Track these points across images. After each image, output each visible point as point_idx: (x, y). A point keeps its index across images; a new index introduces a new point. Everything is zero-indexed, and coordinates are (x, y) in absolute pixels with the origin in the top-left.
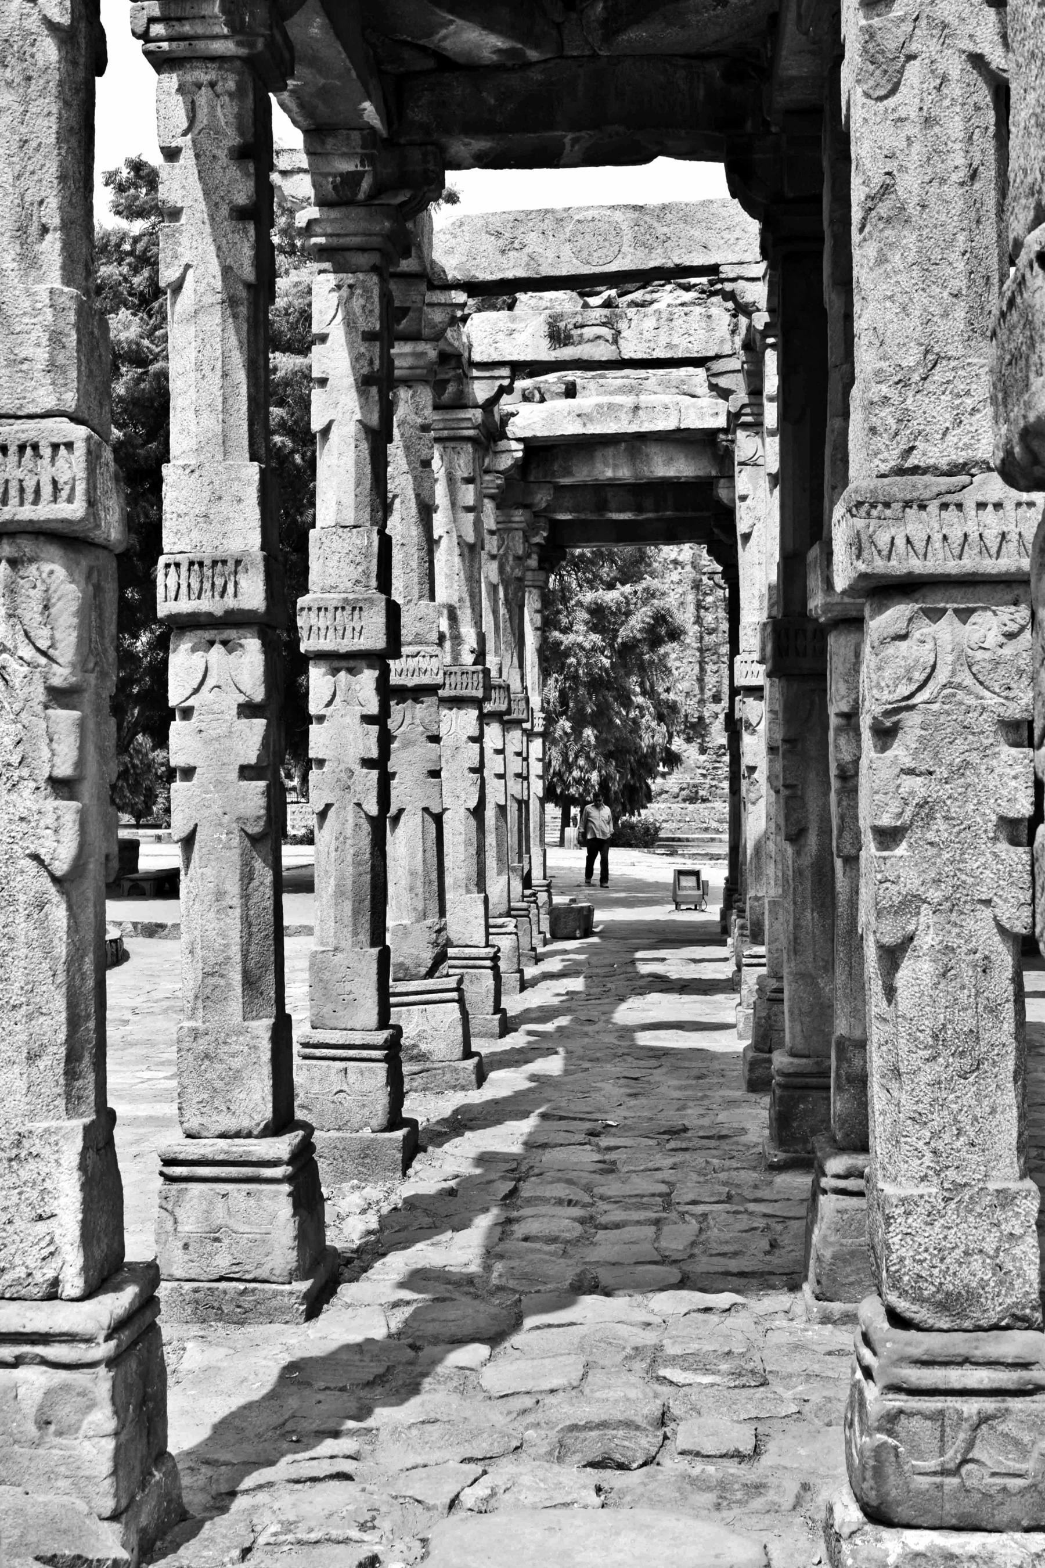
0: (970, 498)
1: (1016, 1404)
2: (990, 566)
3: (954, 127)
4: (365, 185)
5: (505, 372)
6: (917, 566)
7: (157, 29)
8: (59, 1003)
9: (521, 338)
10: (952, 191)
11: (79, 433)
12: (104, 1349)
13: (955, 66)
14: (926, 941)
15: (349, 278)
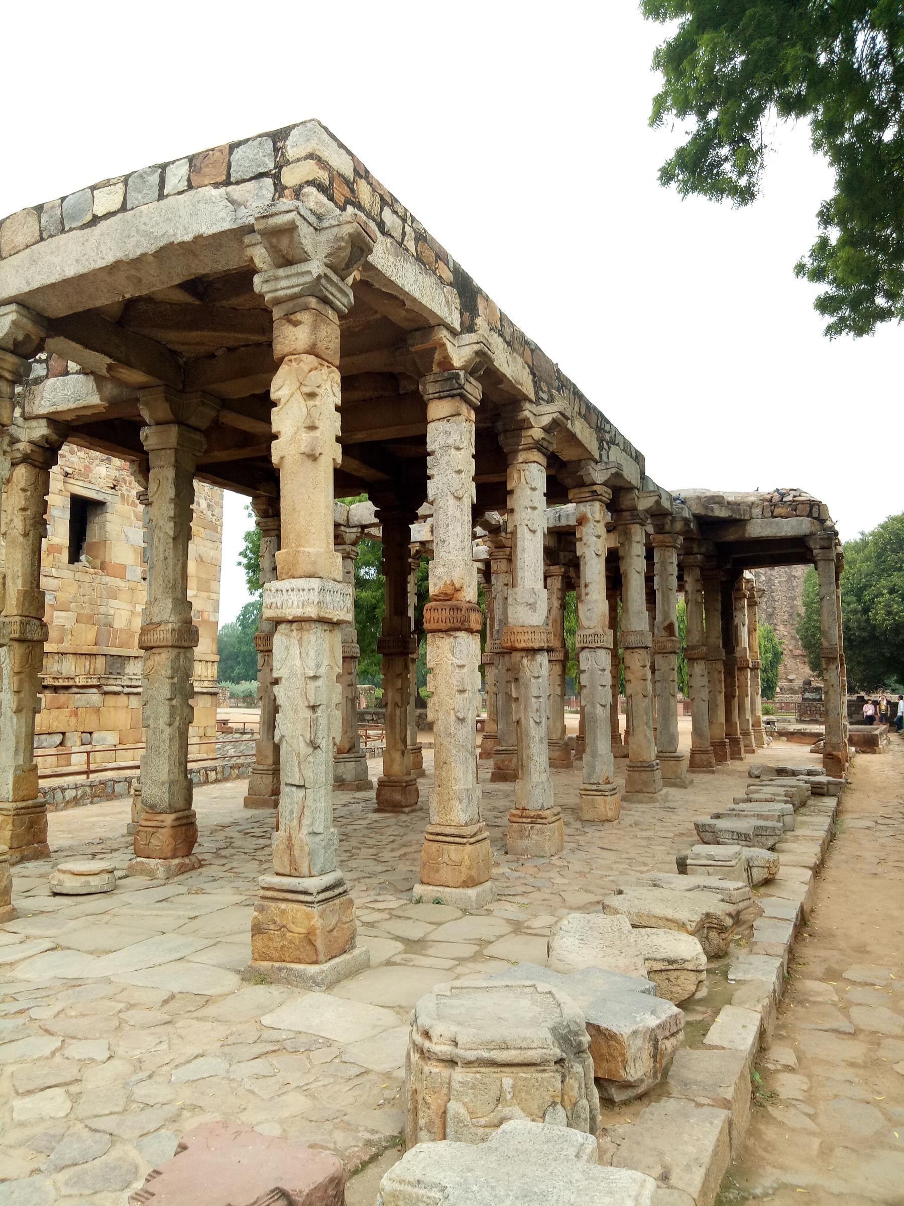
0: (158, 629)
1: (160, 830)
2: (161, 644)
3: (161, 549)
4: (270, 511)
5: (418, 544)
6: (149, 645)
7: (142, 498)
8: (14, 738)
9: (422, 533)
10: (160, 563)
11: (18, 619)
12: (12, 813)
13: (161, 535)
14: (151, 726)
15: (269, 539)
